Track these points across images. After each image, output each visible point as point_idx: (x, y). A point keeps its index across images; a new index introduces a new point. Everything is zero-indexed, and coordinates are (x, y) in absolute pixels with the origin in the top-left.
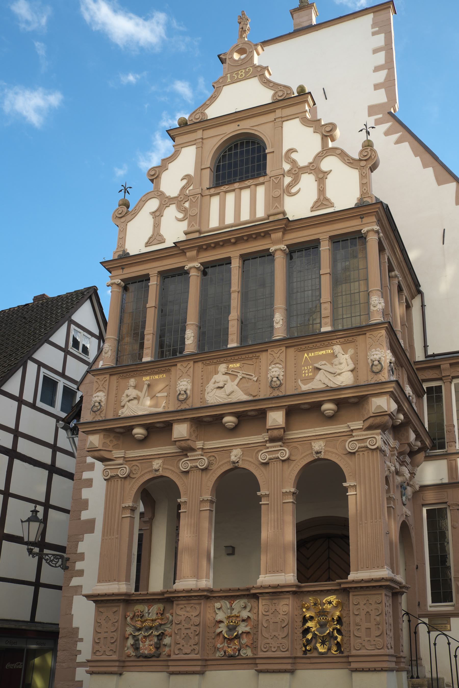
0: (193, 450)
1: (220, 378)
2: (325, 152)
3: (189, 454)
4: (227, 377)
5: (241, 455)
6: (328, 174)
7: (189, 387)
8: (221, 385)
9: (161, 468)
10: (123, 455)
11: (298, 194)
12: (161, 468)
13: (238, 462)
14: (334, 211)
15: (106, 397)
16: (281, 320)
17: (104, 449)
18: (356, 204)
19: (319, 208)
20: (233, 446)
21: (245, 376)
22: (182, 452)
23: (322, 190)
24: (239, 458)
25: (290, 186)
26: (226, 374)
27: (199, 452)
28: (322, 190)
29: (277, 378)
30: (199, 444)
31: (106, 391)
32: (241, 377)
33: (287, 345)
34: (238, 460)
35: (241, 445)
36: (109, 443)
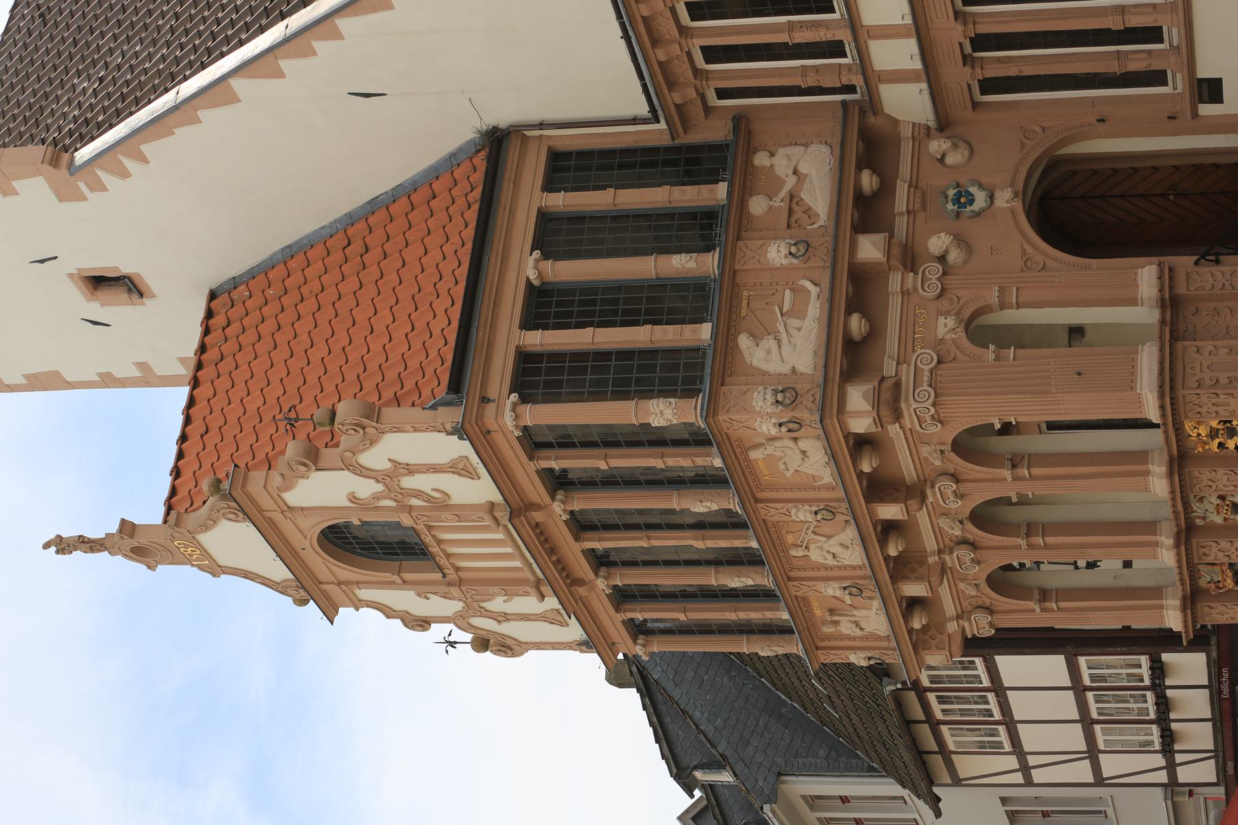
0: (943, 565)
1: (815, 555)
2: (350, 467)
3: (950, 565)
4: (812, 547)
5: (949, 518)
6: (399, 464)
7: (836, 585)
8: (830, 557)
9: (974, 582)
10: (955, 622)
11: (444, 490)
12: (974, 582)
13: (961, 522)
14: (481, 465)
15: (858, 652)
16: (704, 504)
17: (947, 647)
18: (461, 438)
19: (473, 472)
20: (932, 525)
21: (811, 531)
22: (946, 573)
23: (435, 469)
24: (953, 520)
25: (429, 499)
26: (807, 547)
27: (947, 558)
28: (435, 469)
29: (816, 513)
30: (932, 560)
31: (847, 652)
32: (813, 536)
33: (753, 503)
34: (957, 523)
35: (930, 519)
36: (937, 640)
